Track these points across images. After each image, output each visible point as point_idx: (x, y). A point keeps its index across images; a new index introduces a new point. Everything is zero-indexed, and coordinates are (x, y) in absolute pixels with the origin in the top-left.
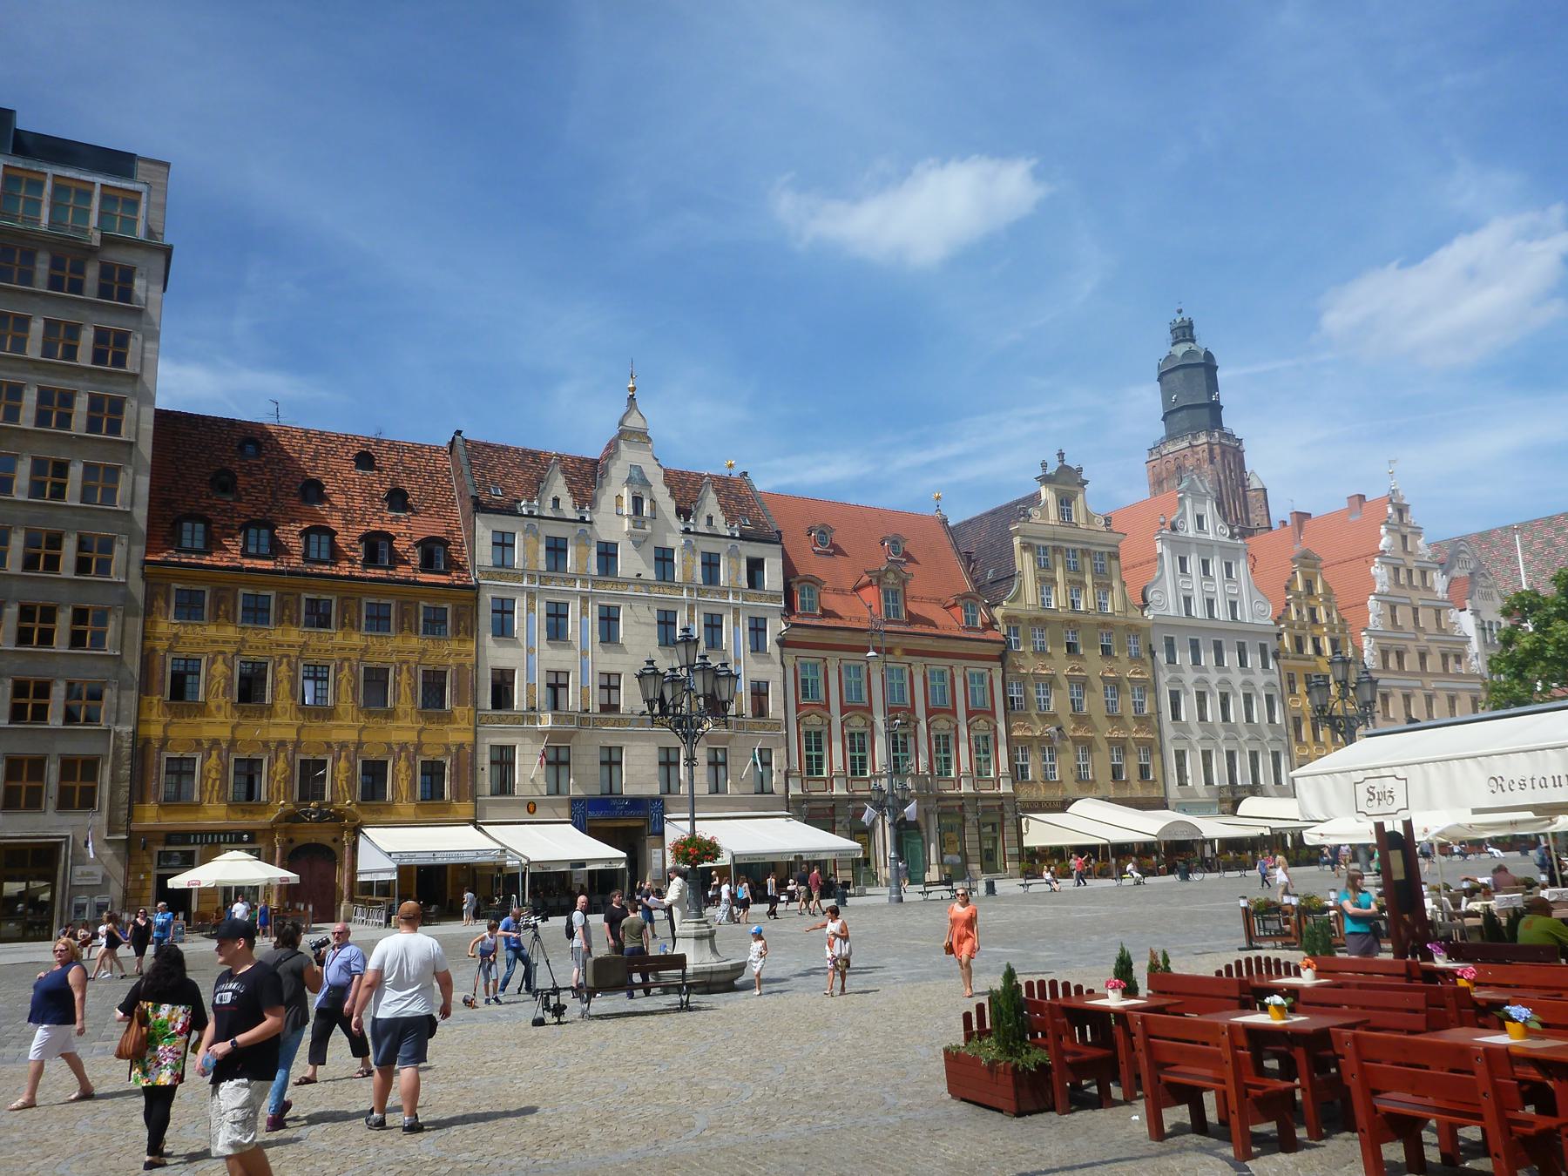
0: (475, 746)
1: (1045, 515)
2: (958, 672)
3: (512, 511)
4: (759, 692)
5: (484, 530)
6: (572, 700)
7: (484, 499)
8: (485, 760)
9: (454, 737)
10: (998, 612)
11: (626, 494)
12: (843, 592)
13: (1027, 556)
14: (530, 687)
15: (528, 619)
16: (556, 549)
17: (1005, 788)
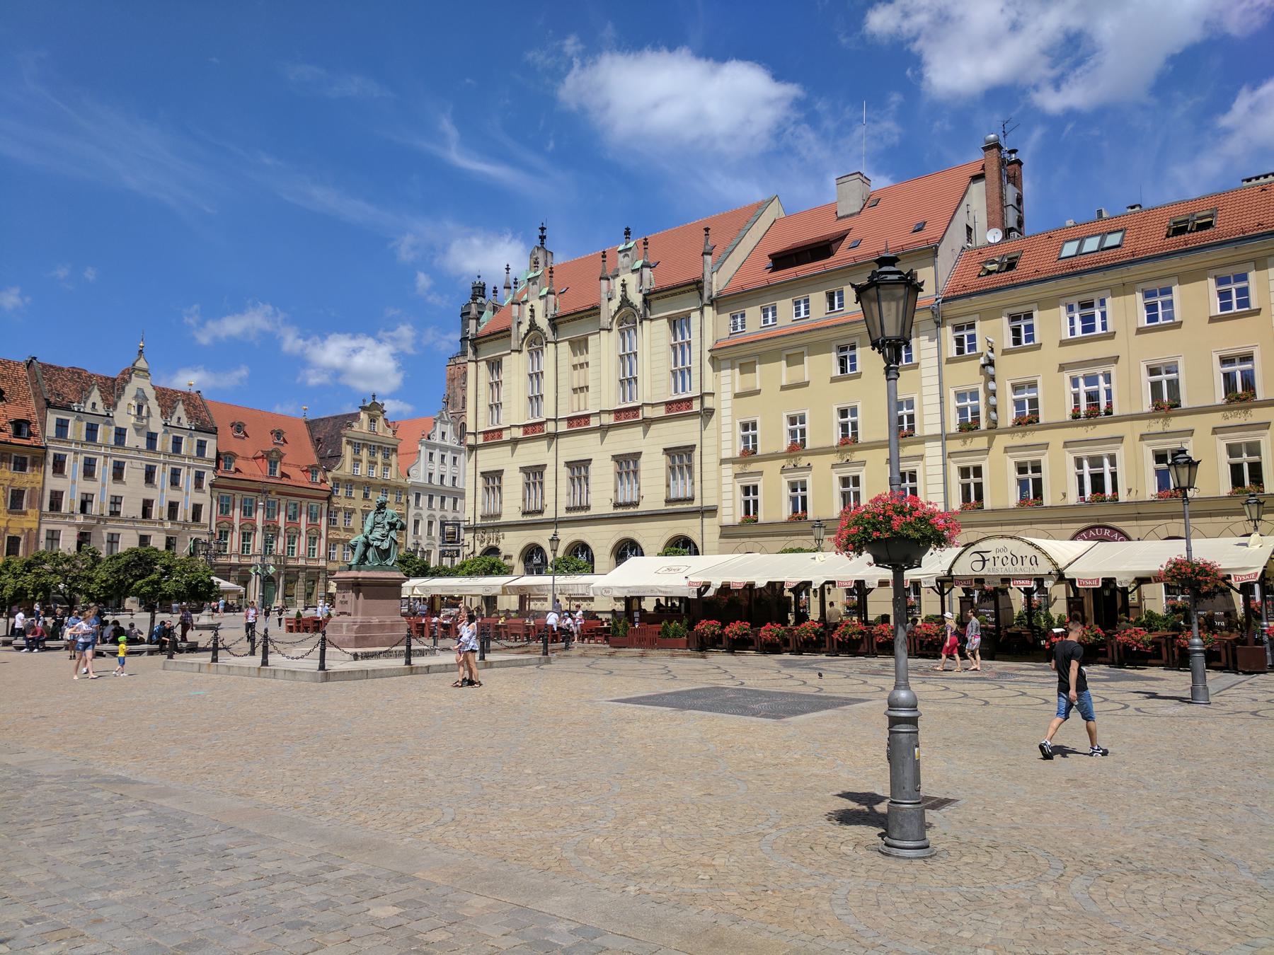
0: (39, 530)
1: (361, 427)
2: (304, 504)
3: (68, 408)
4: (197, 509)
5: (52, 418)
6: (94, 509)
7: (52, 400)
8: (43, 537)
9: (27, 525)
10: (329, 475)
11: (134, 403)
12: (247, 459)
13: (349, 448)
14: (72, 501)
15: (74, 465)
16: (92, 430)
17: (322, 563)
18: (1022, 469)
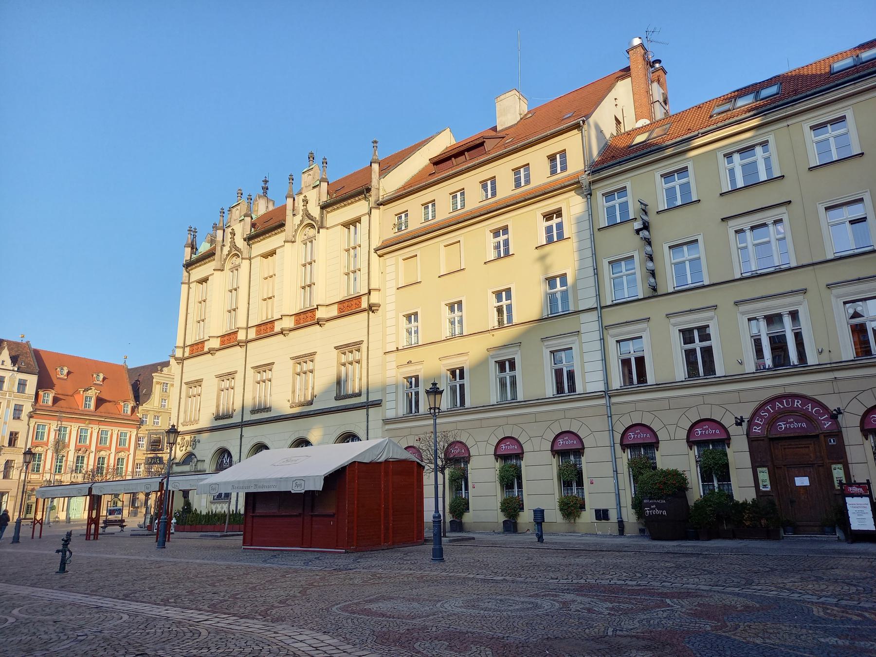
18: (687, 335)
